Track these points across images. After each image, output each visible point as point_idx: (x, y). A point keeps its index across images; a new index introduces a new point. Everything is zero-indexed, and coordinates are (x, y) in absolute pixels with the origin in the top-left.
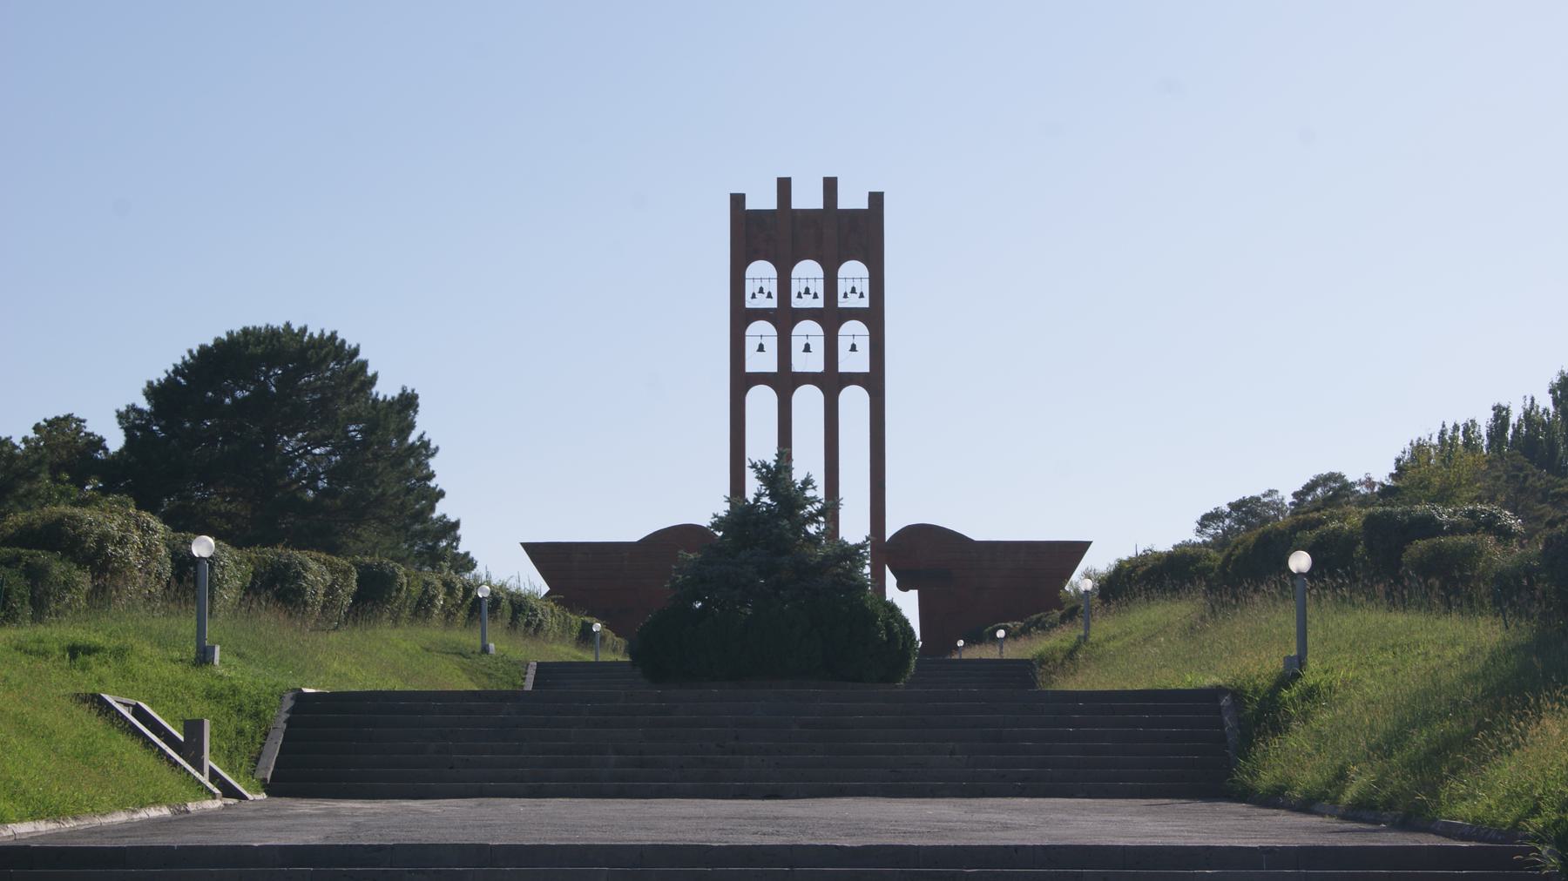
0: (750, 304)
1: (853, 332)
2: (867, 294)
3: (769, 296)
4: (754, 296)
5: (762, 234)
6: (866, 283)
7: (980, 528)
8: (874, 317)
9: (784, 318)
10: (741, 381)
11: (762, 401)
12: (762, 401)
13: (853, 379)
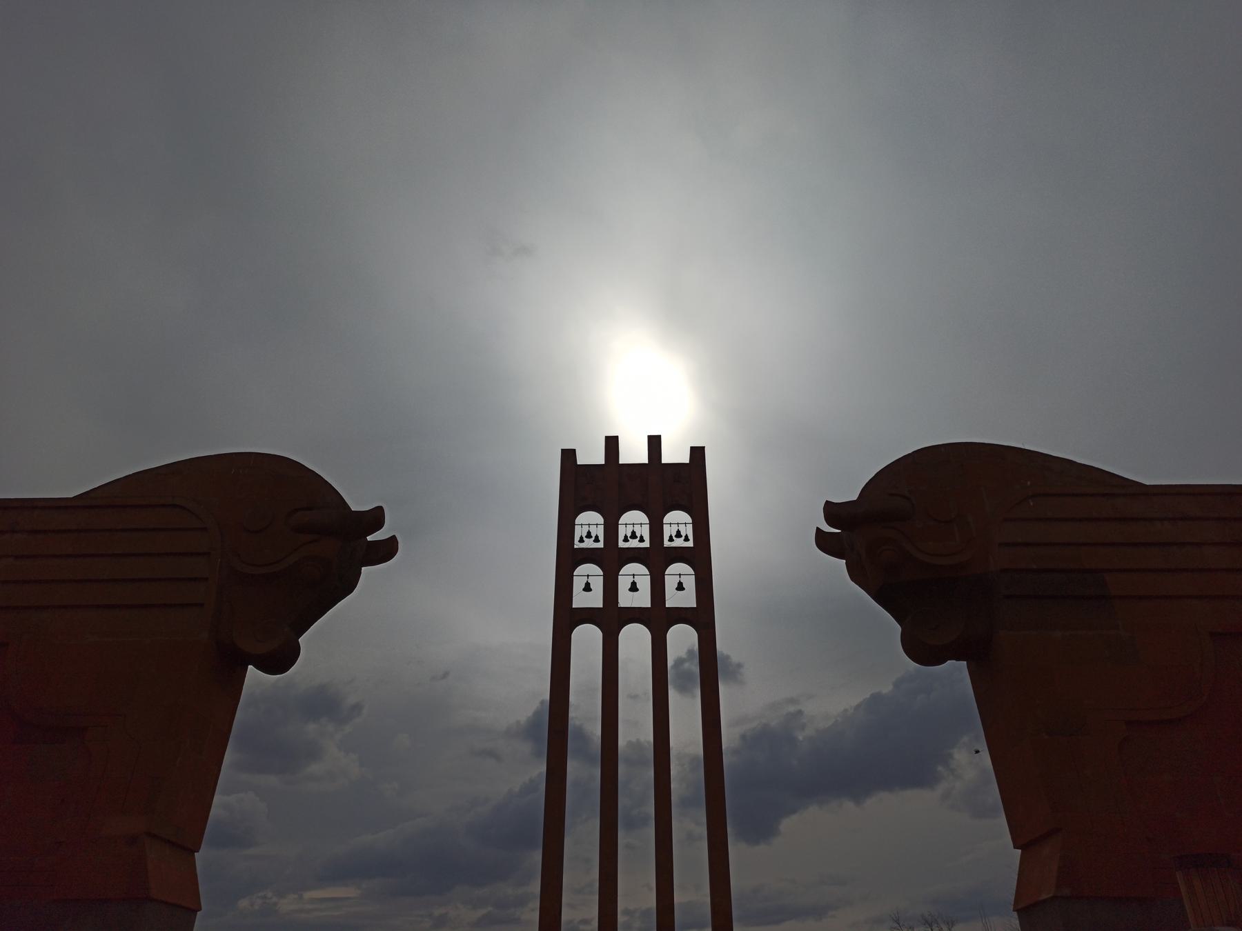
0: (577, 545)
1: (679, 572)
2: (691, 537)
3: (597, 540)
4: (581, 540)
6: (690, 527)
9: (611, 558)
10: (567, 618)
11: (587, 638)
12: (587, 638)
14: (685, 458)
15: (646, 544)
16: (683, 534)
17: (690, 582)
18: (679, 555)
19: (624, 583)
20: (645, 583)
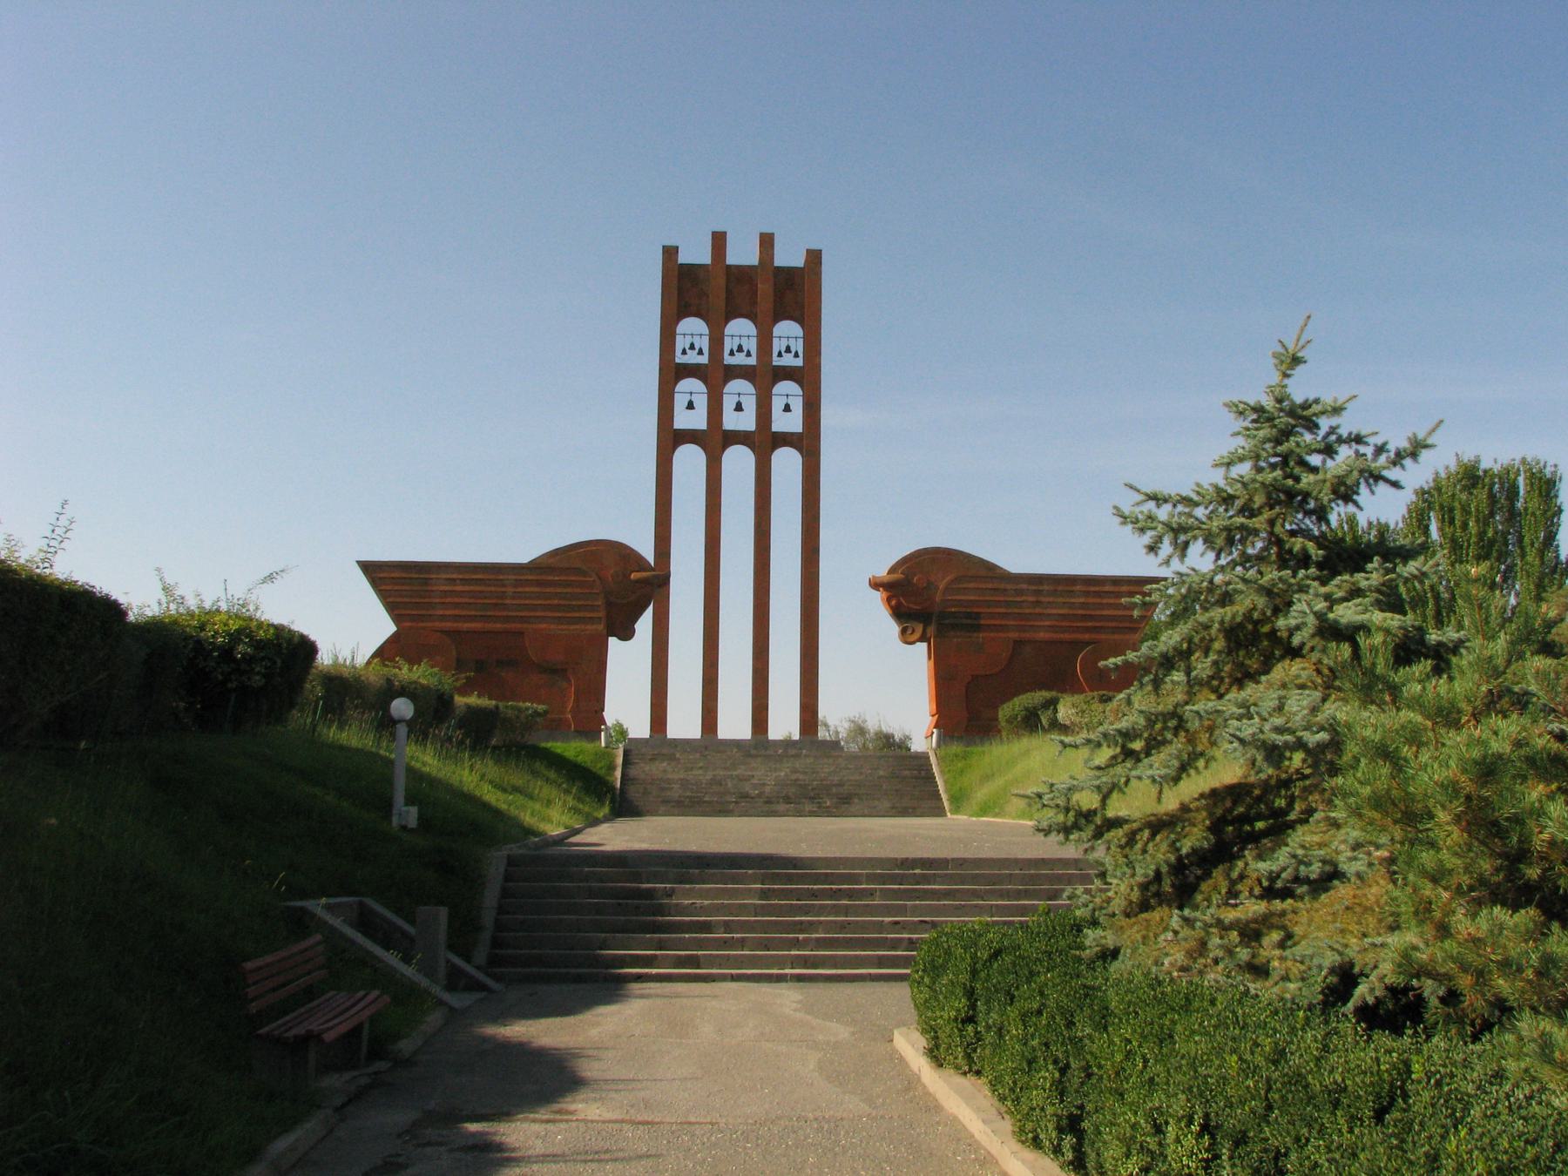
3: (701, 352)
4: (684, 352)
5: (690, 289)
6: (801, 341)
7: (1019, 556)
8: (808, 377)
9: (716, 375)
10: (670, 439)
11: (689, 460)
12: (689, 460)
17: (797, 406)
19: (728, 403)
20: (750, 404)
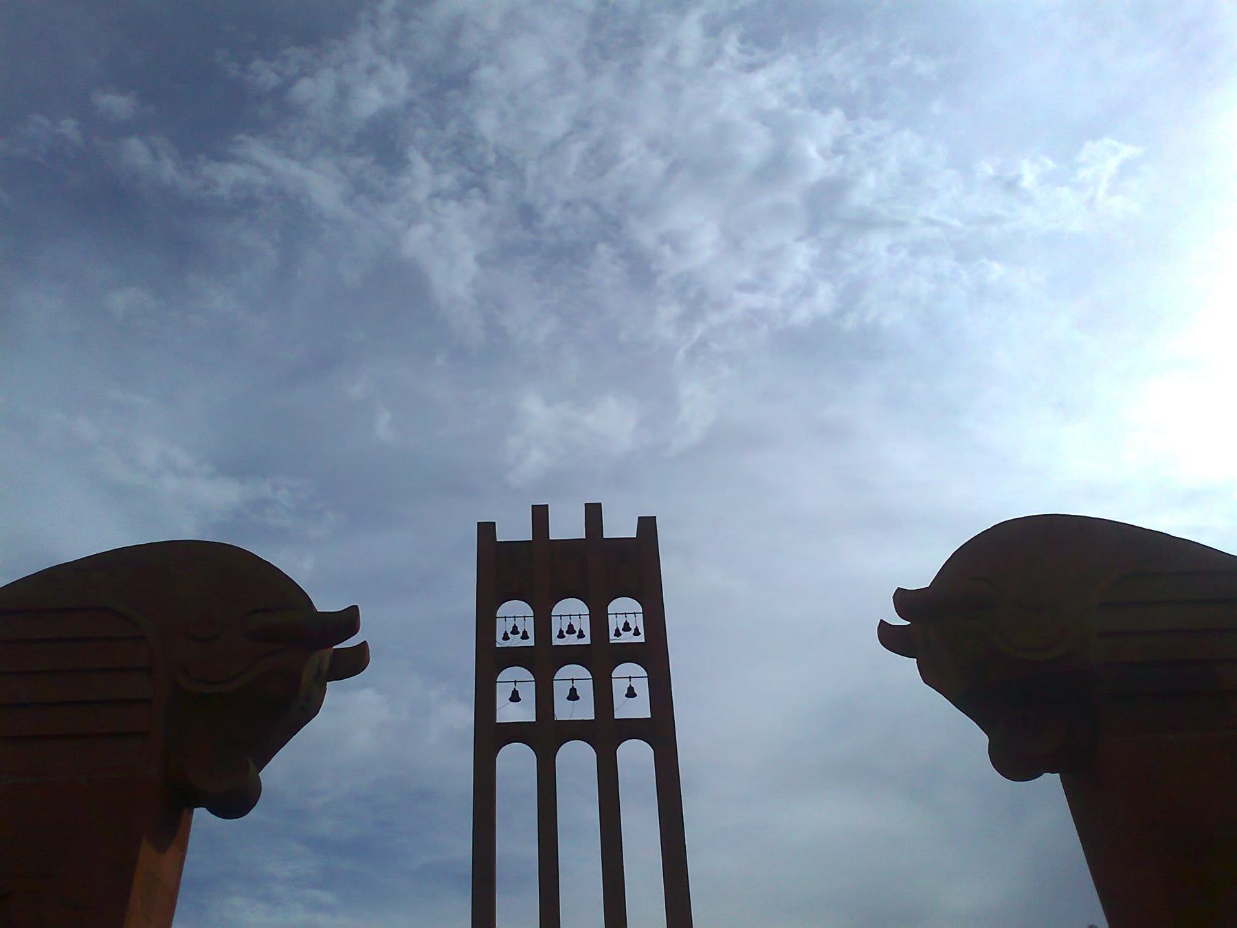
0: (500, 643)
1: (628, 675)
2: (641, 630)
3: (525, 636)
4: (506, 637)
8: (653, 654)
9: (543, 660)
10: (490, 736)
11: (516, 762)
12: (516, 762)
13: (633, 729)
14: (630, 531)
15: (587, 640)
16: (633, 627)
17: (642, 688)
18: (628, 653)
19: (560, 690)
20: (586, 689)
